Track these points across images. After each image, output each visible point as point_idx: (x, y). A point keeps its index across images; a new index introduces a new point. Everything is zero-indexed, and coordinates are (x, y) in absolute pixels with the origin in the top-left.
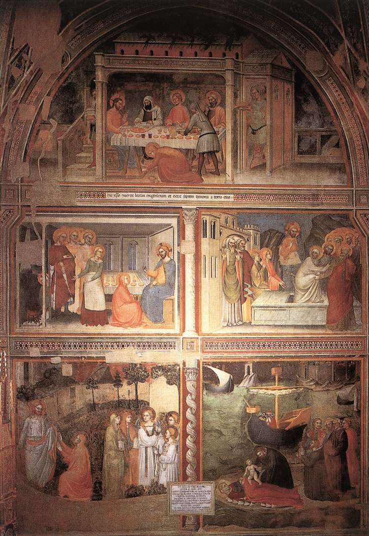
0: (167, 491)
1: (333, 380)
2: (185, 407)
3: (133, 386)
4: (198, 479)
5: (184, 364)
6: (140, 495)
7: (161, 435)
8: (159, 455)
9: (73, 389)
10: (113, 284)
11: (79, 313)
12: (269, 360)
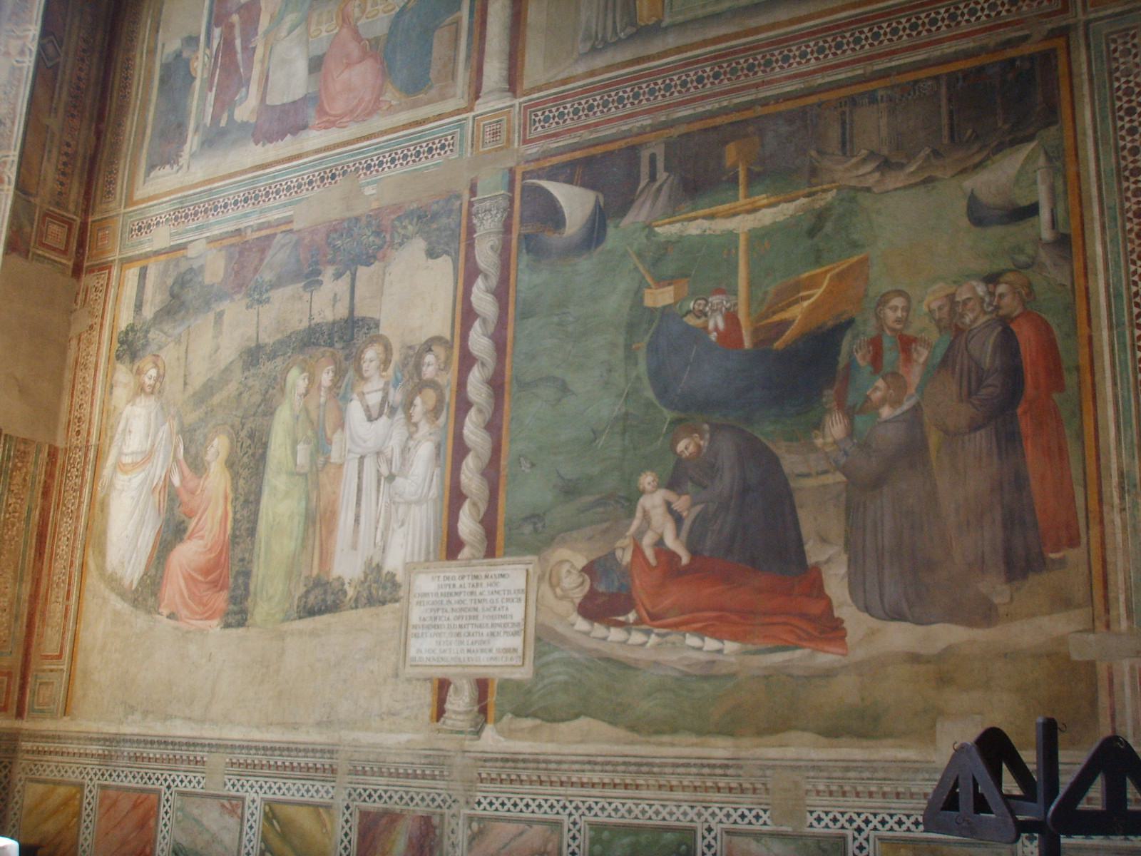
0: (401, 593)
1: (946, 141)
2: (468, 315)
3: (346, 278)
4: (490, 552)
5: (473, 192)
6: (334, 608)
7: (400, 415)
8: (391, 478)
9: (220, 316)
10: (330, 29)
11: (253, 120)
12: (718, 121)
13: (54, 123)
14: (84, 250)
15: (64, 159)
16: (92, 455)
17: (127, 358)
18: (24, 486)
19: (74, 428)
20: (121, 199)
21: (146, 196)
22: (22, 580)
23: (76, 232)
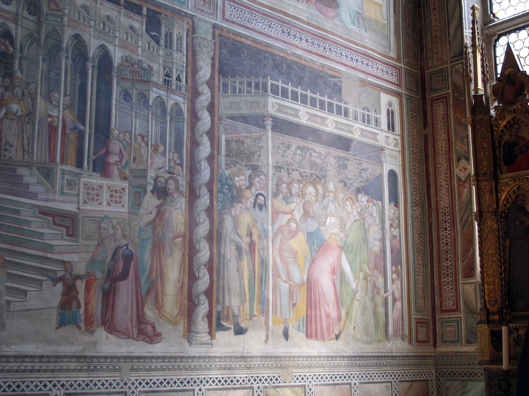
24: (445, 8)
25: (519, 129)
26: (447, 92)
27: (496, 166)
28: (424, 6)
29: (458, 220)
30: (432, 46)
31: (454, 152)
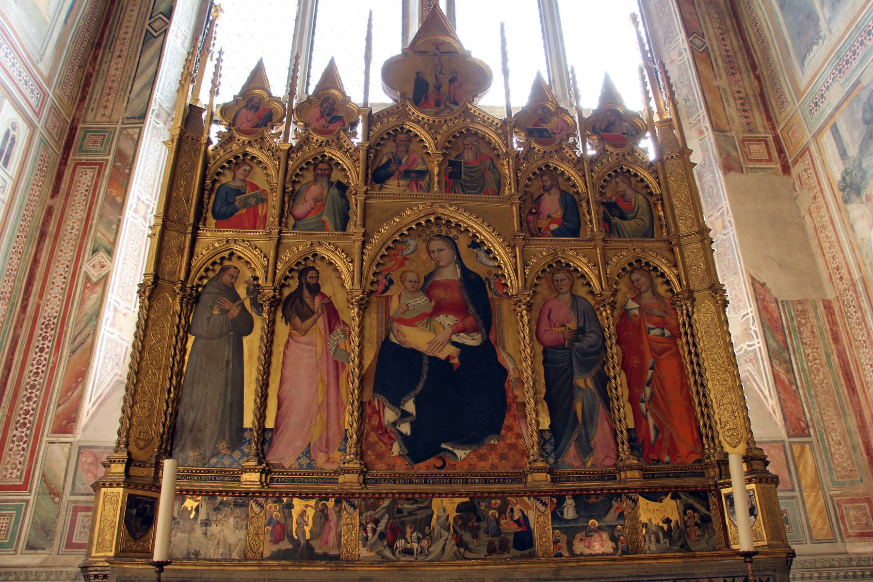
13: (723, 82)
14: (784, 153)
15: (740, 101)
16: (860, 288)
17: (853, 197)
18: (814, 338)
19: (836, 277)
20: (793, 99)
21: (809, 79)
22: (845, 415)
23: (772, 144)
24: (135, 59)
25: (249, 172)
26: (105, 158)
27: (199, 215)
28: (105, 48)
29: (68, 339)
30: (101, 97)
31: (90, 239)
